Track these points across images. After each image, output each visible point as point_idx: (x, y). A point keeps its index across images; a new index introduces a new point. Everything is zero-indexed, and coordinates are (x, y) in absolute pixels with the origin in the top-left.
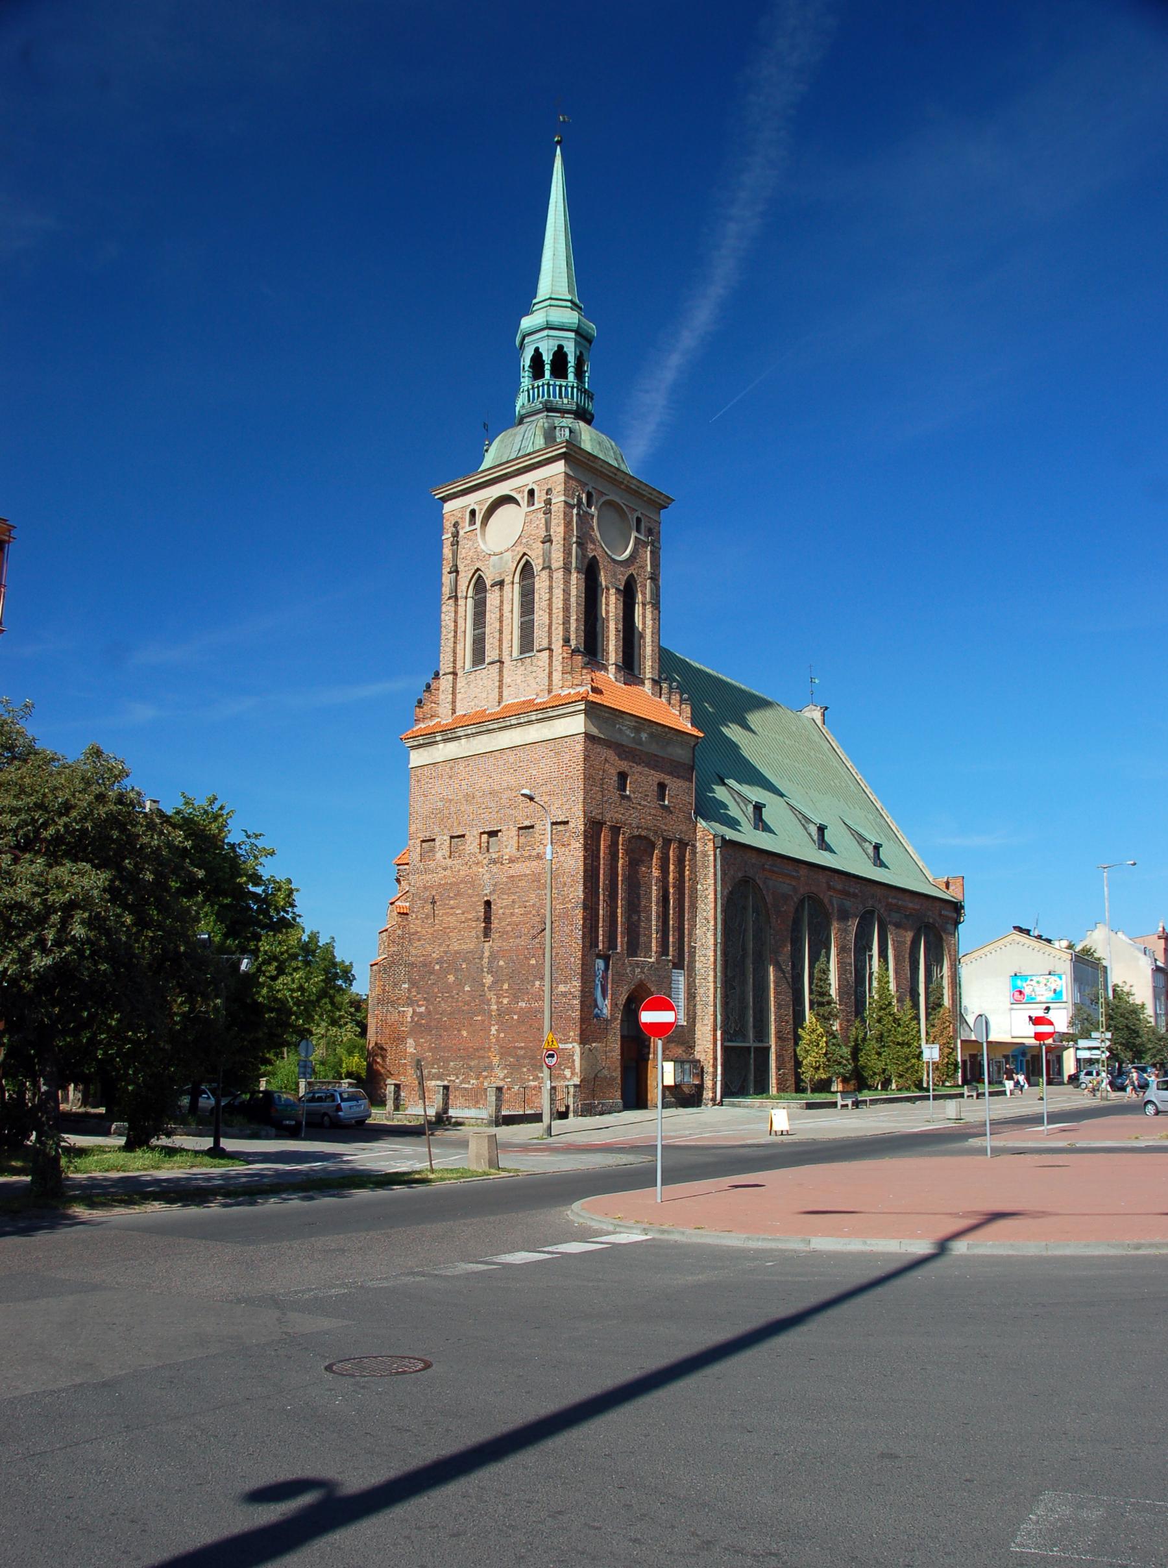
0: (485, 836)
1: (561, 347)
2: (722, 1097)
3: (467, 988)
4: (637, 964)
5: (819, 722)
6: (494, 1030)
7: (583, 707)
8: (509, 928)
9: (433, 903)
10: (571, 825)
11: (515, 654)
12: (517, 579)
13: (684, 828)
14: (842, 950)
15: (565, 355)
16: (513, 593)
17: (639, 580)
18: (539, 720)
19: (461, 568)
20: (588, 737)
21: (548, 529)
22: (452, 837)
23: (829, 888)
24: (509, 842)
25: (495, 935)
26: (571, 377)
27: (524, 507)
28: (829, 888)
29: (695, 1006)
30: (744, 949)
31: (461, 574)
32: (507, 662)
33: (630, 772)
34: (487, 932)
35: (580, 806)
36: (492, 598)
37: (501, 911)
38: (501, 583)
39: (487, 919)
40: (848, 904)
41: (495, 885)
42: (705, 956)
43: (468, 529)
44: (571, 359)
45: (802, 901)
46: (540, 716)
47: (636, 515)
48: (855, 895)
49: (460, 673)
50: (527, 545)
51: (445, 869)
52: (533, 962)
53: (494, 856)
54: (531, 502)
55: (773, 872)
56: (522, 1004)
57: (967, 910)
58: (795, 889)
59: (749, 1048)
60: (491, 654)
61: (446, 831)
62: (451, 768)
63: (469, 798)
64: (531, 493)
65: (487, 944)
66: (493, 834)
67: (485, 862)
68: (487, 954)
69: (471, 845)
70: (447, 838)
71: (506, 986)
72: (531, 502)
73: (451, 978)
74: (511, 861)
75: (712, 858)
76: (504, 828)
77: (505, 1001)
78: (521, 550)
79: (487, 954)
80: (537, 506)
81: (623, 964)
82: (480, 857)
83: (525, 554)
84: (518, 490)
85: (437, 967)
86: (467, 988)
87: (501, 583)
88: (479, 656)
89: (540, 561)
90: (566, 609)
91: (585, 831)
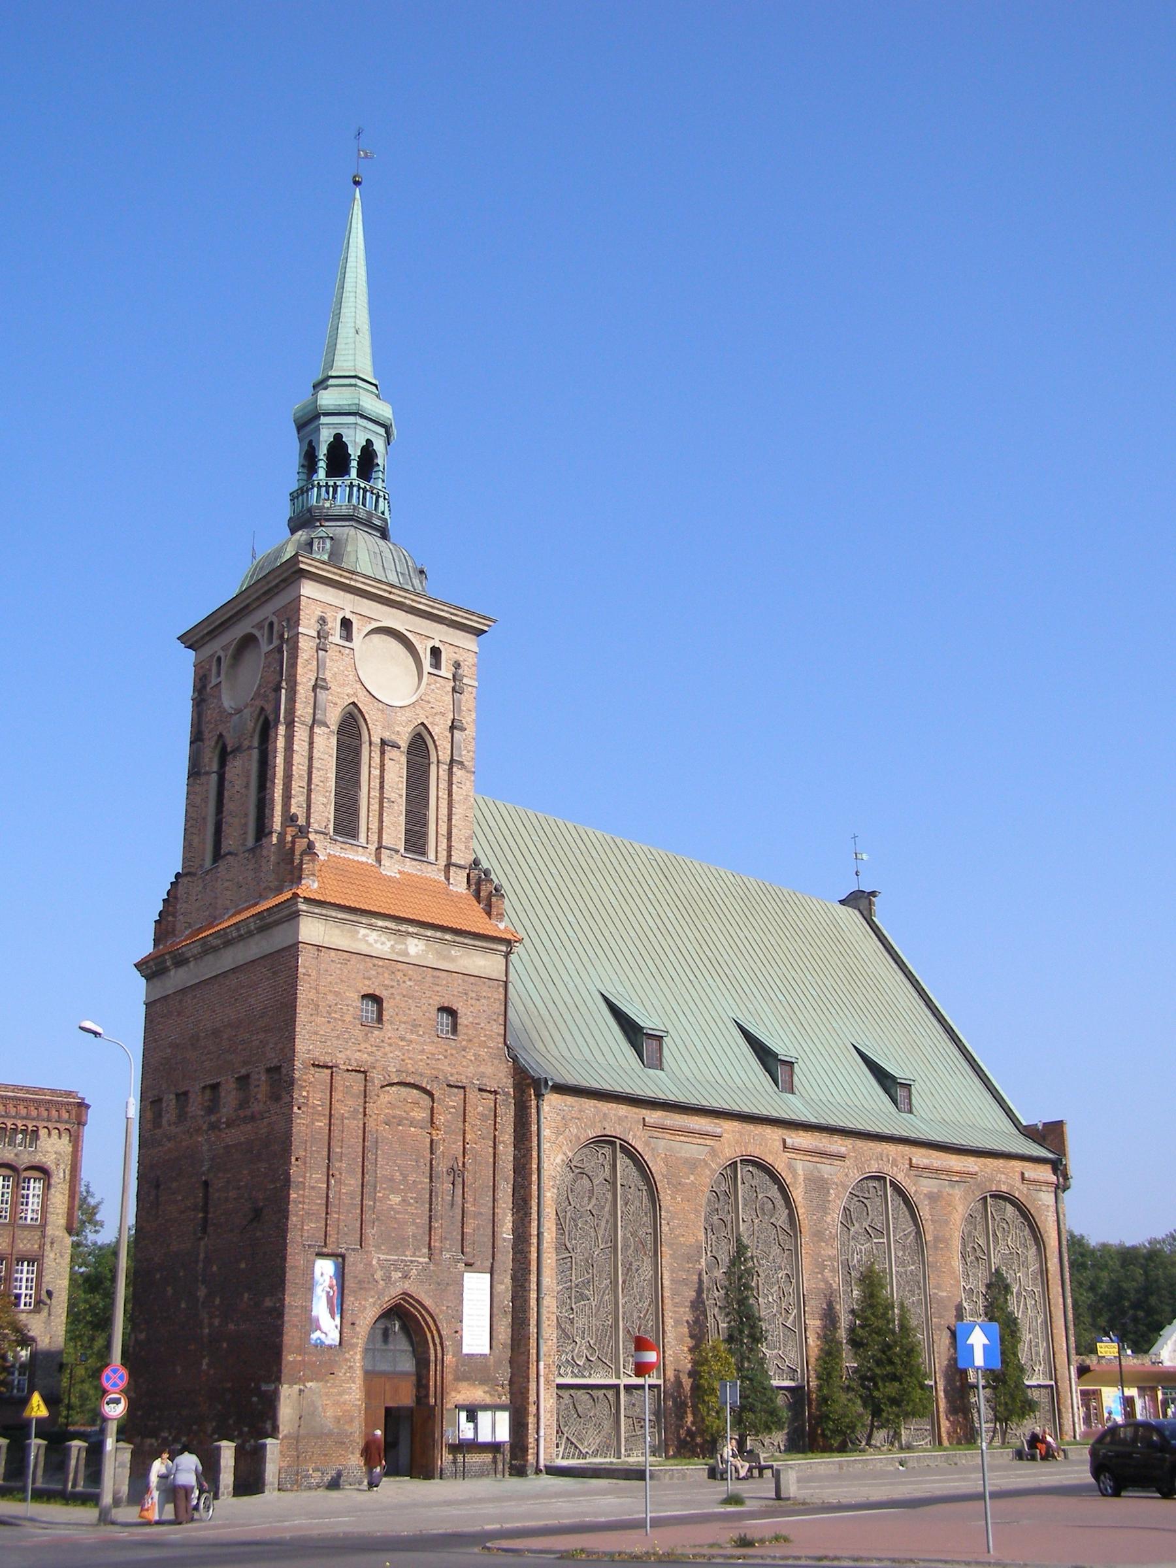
0: (208, 1092)
1: (338, 437)
3: (183, 1306)
4: (395, 1265)
5: (865, 913)
6: (205, 1362)
9: (158, 1186)
13: (489, 1070)
15: (345, 446)
19: (206, 735)
22: (177, 1095)
24: (229, 1097)
25: (210, 1229)
26: (354, 473)
31: (207, 743)
37: (217, 1195)
40: (827, 1169)
41: (212, 1159)
43: (214, 682)
44: (354, 452)
47: (430, 644)
48: (842, 1157)
50: (265, 696)
51: (169, 1139)
52: (243, 1266)
54: (270, 641)
56: (231, 1326)
57: (1072, 1170)
58: (713, 1152)
61: (172, 1088)
62: (181, 1001)
66: (215, 1087)
67: (205, 1127)
68: (202, 1256)
70: (172, 1096)
72: (270, 641)
73: (170, 1290)
74: (229, 1125)
76: (222, 1079)
77: (217, 1322)
78: (259, 703)
79: (202, 1256)
81: (370, 1264)
83: (262, 709)
84: (259, 626)
85: (158, 1276)
86: (183, 1306)
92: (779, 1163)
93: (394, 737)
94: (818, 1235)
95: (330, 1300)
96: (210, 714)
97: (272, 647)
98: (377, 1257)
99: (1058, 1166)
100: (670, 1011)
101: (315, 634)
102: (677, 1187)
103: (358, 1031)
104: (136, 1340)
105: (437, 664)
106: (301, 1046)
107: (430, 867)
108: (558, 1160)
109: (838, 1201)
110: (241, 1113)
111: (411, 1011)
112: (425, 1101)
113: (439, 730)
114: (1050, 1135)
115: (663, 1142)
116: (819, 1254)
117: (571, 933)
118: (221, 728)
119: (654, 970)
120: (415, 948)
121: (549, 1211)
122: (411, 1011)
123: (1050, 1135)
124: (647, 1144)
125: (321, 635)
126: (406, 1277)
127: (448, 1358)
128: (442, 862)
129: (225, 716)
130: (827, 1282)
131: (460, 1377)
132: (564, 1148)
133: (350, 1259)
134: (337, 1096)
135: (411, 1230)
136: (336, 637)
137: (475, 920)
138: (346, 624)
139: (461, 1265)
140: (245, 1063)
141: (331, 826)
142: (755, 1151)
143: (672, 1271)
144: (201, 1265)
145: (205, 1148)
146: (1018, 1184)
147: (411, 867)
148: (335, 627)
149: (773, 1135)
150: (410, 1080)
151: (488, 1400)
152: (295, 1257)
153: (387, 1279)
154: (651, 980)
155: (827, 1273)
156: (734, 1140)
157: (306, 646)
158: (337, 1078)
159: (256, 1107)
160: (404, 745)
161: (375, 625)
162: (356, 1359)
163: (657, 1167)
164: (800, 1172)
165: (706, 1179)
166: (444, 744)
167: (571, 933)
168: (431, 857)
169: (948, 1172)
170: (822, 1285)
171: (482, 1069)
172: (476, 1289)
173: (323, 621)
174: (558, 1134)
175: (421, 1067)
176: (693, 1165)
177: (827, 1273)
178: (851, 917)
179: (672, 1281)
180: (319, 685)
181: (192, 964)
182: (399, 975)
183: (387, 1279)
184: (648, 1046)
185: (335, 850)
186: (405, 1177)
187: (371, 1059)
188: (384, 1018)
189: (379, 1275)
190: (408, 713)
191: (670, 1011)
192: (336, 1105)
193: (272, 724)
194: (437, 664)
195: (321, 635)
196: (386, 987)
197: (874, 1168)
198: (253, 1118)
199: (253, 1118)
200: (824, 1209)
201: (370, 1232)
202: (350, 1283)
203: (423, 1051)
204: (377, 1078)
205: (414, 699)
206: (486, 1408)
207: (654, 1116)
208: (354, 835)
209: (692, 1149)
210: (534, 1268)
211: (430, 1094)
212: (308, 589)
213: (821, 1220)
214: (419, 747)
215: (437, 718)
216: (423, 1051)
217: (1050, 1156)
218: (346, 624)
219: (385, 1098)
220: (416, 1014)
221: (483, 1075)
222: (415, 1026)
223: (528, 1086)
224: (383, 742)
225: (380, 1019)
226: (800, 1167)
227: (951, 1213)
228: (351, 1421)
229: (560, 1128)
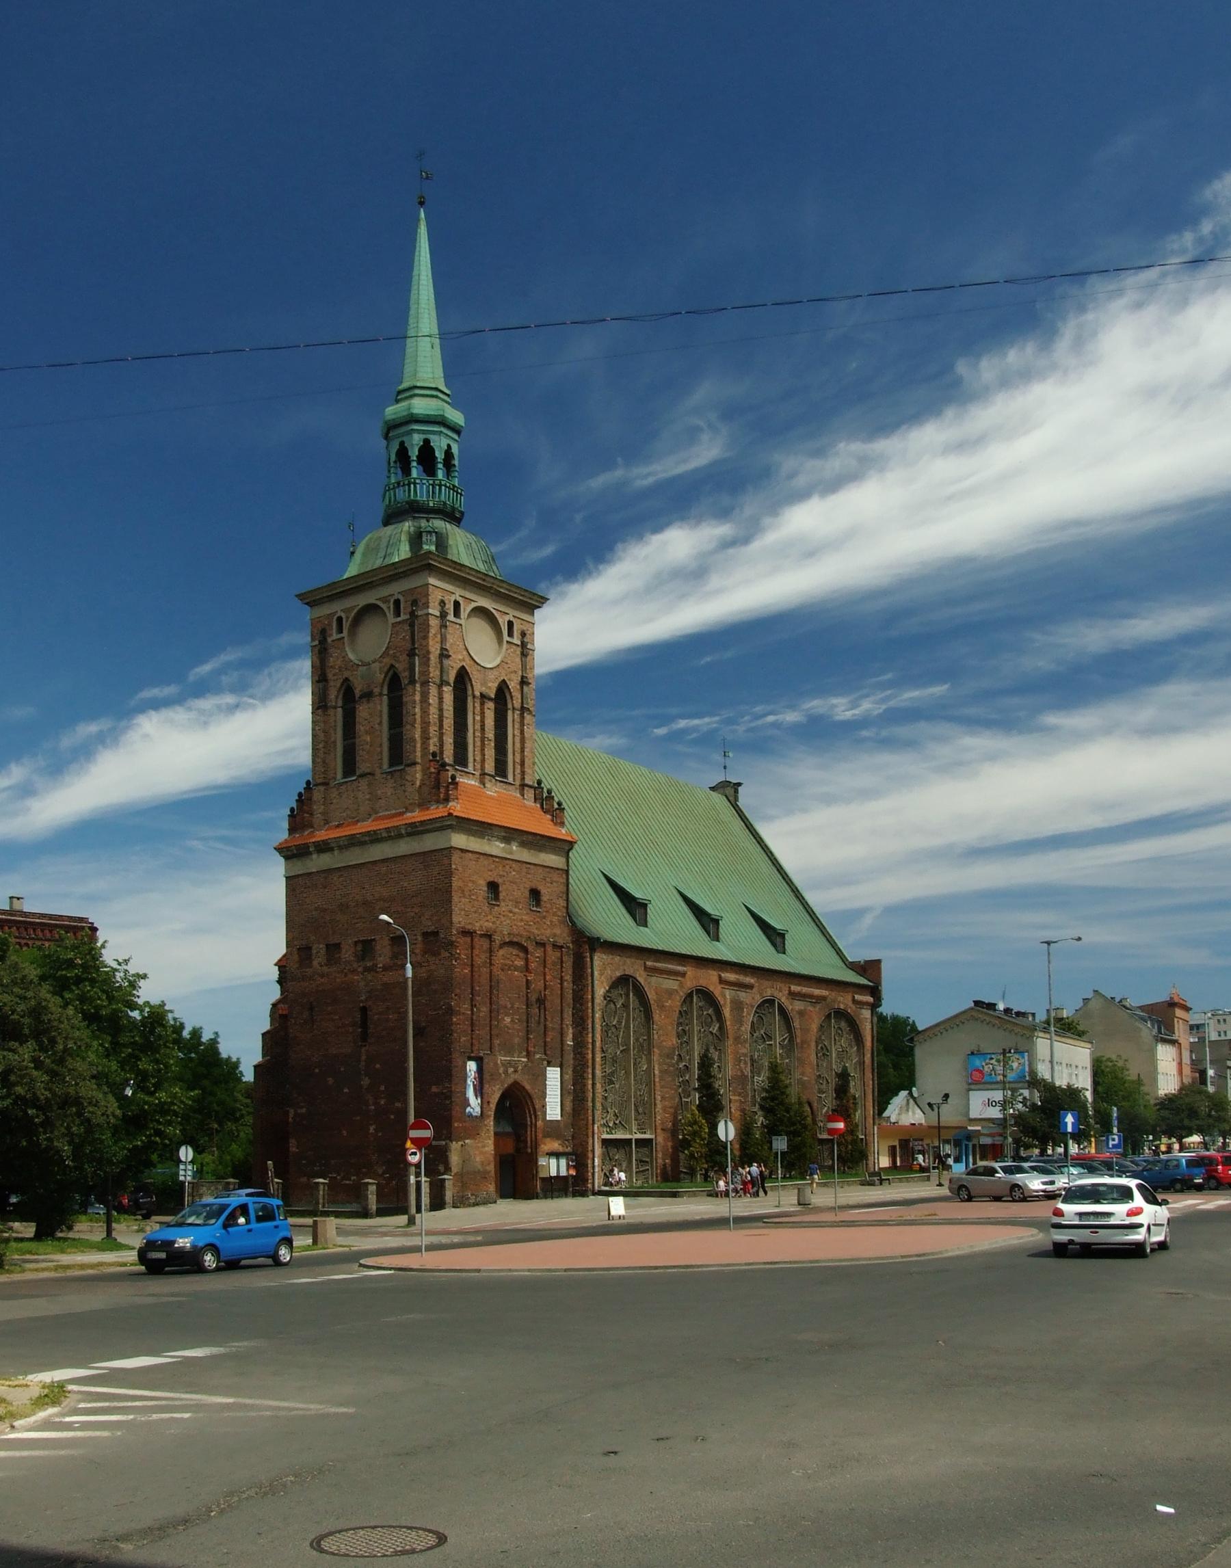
0: (359, 948)
4: (510, 1063)
8: (384, 1033)
9: (311, 1009)
11: (385, 766)
12: (385, 692)
13: (558, 931)
14: (737, 1039)
16: (383, 705)
21: (413, 643)
23: (721, 981)
27: (392, 619)
32: (378, 776)
33: (500, 881)
34: (364, 1037)
36: (363, 711)
39: (364, 1023)
40: (743, 996)
45: (690, 995)
47: (507, 618)
48: (751, 987)
49: (332, 784)
50: (394, 657)
51: (322, 976)
53: (369, 964)
54: (397, 613)
58: (681, 985)
60: (362, 767)
63: (343, 907)
64: (397, 602)
65: (363, 1050)
67: (360, 969)
68: (364, 1058)
69: (347, 953)
71: (382, 1088)
72: (397, 613)
73: (330, 1081)
76: (377, 937)
78: (387, 660)
79: (364, 1058)
80: (403, 617)
81: (496, 1064)
82: (355, 965)
83: (392, 666)
84: (385, 600)
88: (350, 766)
89: (407, 674)
92: (717, 990)
94: (737, 1039)
96: (334, 660)
97: (399, 619)
98: (501, 1058)
99: (875, 991)
101: (438, 614)
102: (662, 1007)
104: (296, 1114)
105: (510, 634)
106: (455, 919)
109: (749, 1017)
111: (513, 892)
112: (522, 955)
114: (870, 969)
118: (346, 674)
121: (598, 1027)
122: (513, 892)
123: (870, 969)
125: (443, 615)
128: (518, 783)
129: (349, 665)
133: (486, 1060)
134: (476, 952)
135: (516, 1040)
136: (451, 617)
137: (543, 825)
138: (457, 605)
142: (703, 982)
143: (659, 1064)
144: (363, 1063)
145: (362, 984)
146: (850, 1004)
148: (450, 608)
152: (457, 1059)
153: (506, 1072)
155: (742, 1065)
156: (694, 977)
157: (434, 623)
158: (476, 939)
161: (473, 605)
163: (651, 995)
165: (675, 1003)
166: (517, 695)
169: (811, 996)
173: (442, 603)
176: (670, 993)
177: (742, 1065)
178: (718, 799)
179: (660, 1071)
180: (444, 655)
181: (336, 852)
183: (506, 1072)
184: (638, 912)
186: (512, 1004)
188: (502, 896)
189: (501, 1070)
192: (476, 958)
193: (405, 681)
194: (510, 634)
195: (443, 615)
196: (501, 876)
201: (496, 1042)
202: (486, 1076)
209: (670, 984)
210: (590, 1064)
211: (525, 950)
212: (432, 581)
217: (865, 982)
218: (457, 605)
219: (501, 952)
221: (555, 935)
223: (586, 943)
227: (811, 1022)
229: (603, 971)
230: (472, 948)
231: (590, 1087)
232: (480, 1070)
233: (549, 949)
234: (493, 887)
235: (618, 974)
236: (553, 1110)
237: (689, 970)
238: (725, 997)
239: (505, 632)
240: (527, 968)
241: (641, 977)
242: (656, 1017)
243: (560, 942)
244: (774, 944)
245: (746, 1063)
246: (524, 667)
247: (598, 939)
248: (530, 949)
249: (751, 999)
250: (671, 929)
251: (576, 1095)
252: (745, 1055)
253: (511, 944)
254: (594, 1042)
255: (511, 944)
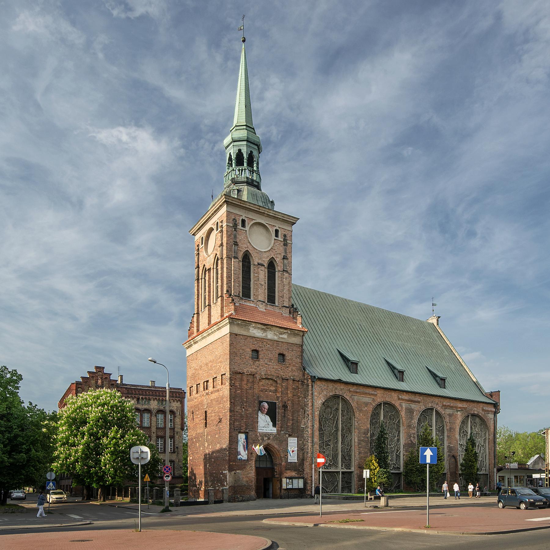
2: (315, 494)
7: (228, 321)
10: (226, 375)
13: (297, 374)
14: (409, 426)
17: (277, 260)
18: (218, 329)
20: (231, 334)
24: (210, 384)
28: (399, 399)
29: (304, 453)
30: (337, 427)
33: (260, 349)
35: (228, 366)
38: (209, 269)
40: (413, 406)
42: (307, 431)
46: (217, 328)
48: (419, 402)
55: (356, 392)
59: (338, 473)
75: (310, 387)
81: (257, 435)
87: (209, 269)
90: (229, 277)
91: (230, 378)
92: (397, 404)
93: (262, 262)
94: (409, 426)
95: (244, 446)
100: (361, 355)
103: (251, 362)
107: (276, 308)
108: (320, 402)
110: (215, 389)
113: (278, 260)
115: (356, 398)
116: (409, 433)
117: (328, 330)
119: (357, 342)
120: (270, 335)
124: (351, 397)
126: (269, 439)
127: (283, 463)
128: (280, 306)
130: (412, 441)
131: (287, 469)
132: (322, 399)
139: (287, 435)
140: (215, 373)
141: (241, 294)
142: (388, 399)
143: (358, 437)
147: (269, 308)
149: (395, 395)
150: (269, 377)
151: (296, 475)
153: (263, 439)
154: (356, 345)
159: (219, 387)
160: (266, 265)
162: (253, 463)
163: (354, 405)
164: (404, 406)
165: (371, 408)
167: (328, 330)
168: (277, 304)
170: (410, 442)
171: (294, 373)
172: (293, 443)
174: (320, 394)
175: (273, 373)
176: (366, 404)
182: (265, 343)
183: (263, 439)
185: (243, 302)
187: (255, 371)
188: (260, 357)
189: (260, 438)
190: (267, 254)
191: (361, 355)
196: (260, 347)
197: (430, 406)
198: (218, 391)
199: (218, 391)
200: (412, 418)
202: (250, 441)
203: (273, 368)
204: (258, 377)
205: (269, 248)
206: (295, 478)
207: (353, 389)
208: (250, 298)
209: (367, 399)
211: (276, 382)
213: (410, 422)
214: (271, 265)
215: (278, 255)
216: (273, 368)
219: (261, 383)
220: (270, 356)
222: (270, 360)
224: (259, 264)
225: (258, 358)
226: (404, 405)
228: (252, 481)
230: (242, 380)
231: (310, 447)
232: (247, 438)
233: (291, 382)
234: (256, 351)
235: (331, 394)
236: (293, 458)
237: (379, 393)
238: (403, 407)
239: (274, 235)
240: (276, 391)
241: (347, 396)
242: (357, 414)
243: (298, 379)
244: (439, 384)
245: (414, 437)
246: (286, 252)
247: (315, 377)
248: (279, 382)
249: (418, 408)
250: (374, 374)
251: (301, 449)
252: (414, 434)
253: (267, 379)
254: (313, 426)
255: (267, 379)
